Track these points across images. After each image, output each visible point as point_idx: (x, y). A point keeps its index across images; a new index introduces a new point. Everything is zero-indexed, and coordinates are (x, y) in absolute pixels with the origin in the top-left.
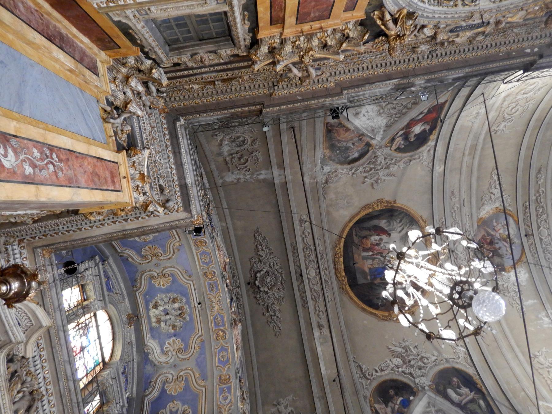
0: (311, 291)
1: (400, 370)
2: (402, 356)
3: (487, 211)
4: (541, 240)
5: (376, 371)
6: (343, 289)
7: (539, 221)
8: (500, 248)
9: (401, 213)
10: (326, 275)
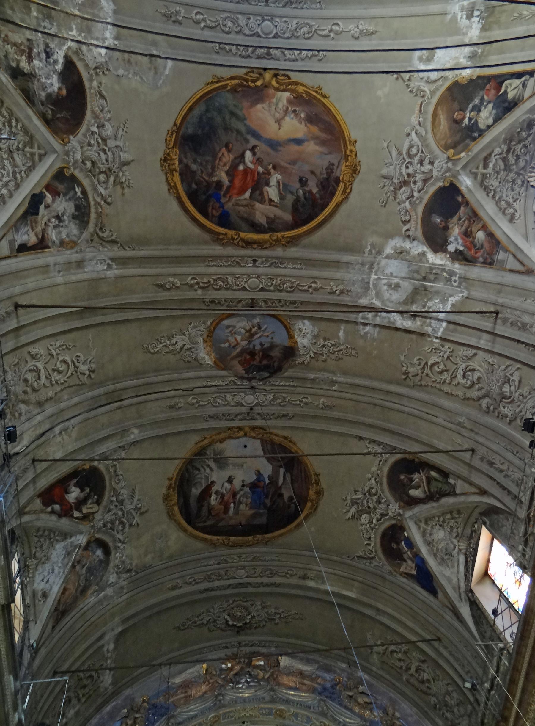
0: (261, 577)
1: (374, 521)
2: (360, 511)
3: (206, 356)
4: (262, 290)
5: (368, 544)
6: (268, 541)
7: (235, 287)
8: (262, 344)
9: (187, 470)
10: (247, 557)
